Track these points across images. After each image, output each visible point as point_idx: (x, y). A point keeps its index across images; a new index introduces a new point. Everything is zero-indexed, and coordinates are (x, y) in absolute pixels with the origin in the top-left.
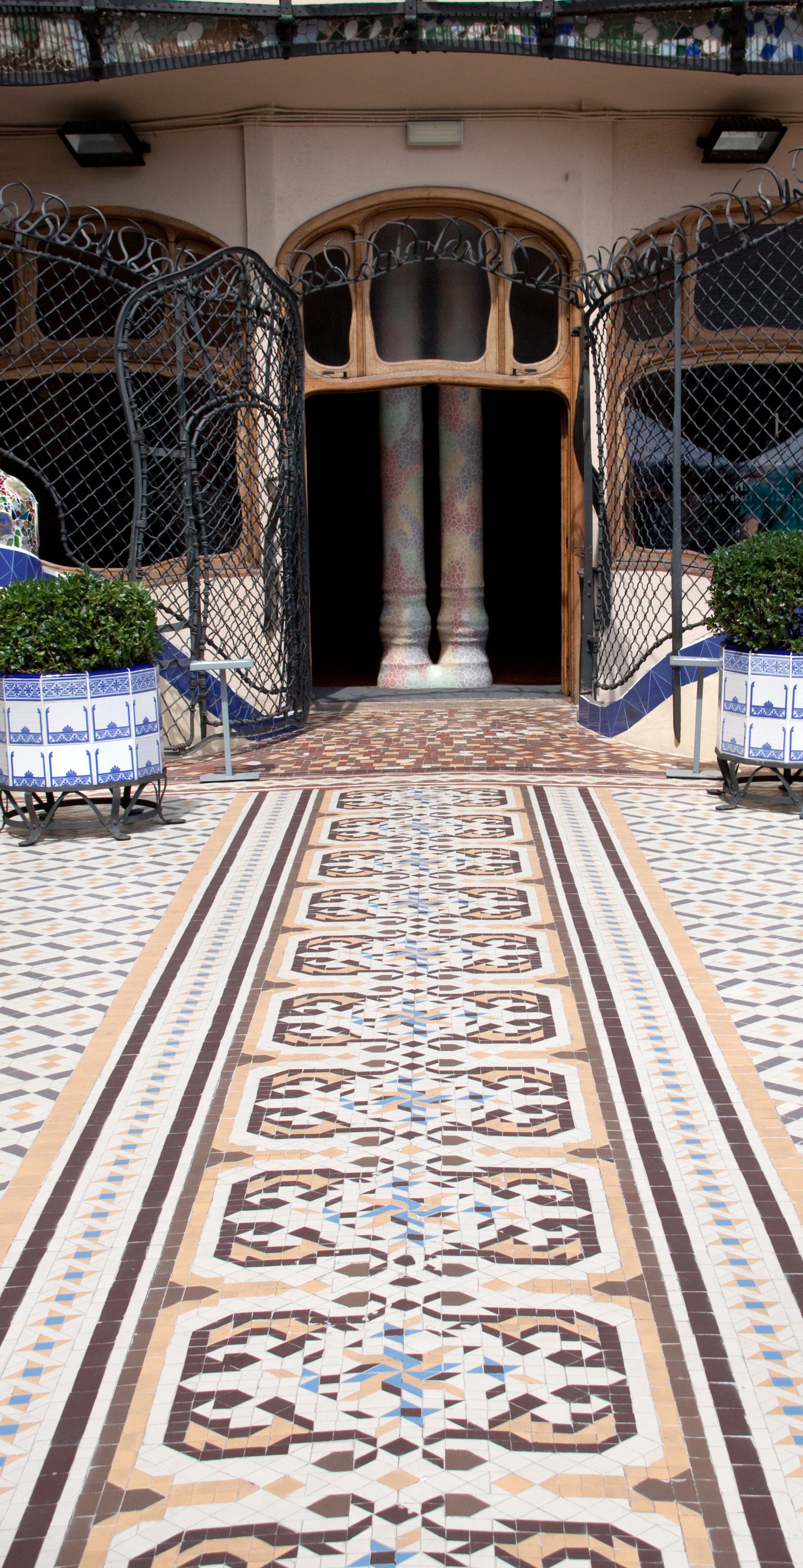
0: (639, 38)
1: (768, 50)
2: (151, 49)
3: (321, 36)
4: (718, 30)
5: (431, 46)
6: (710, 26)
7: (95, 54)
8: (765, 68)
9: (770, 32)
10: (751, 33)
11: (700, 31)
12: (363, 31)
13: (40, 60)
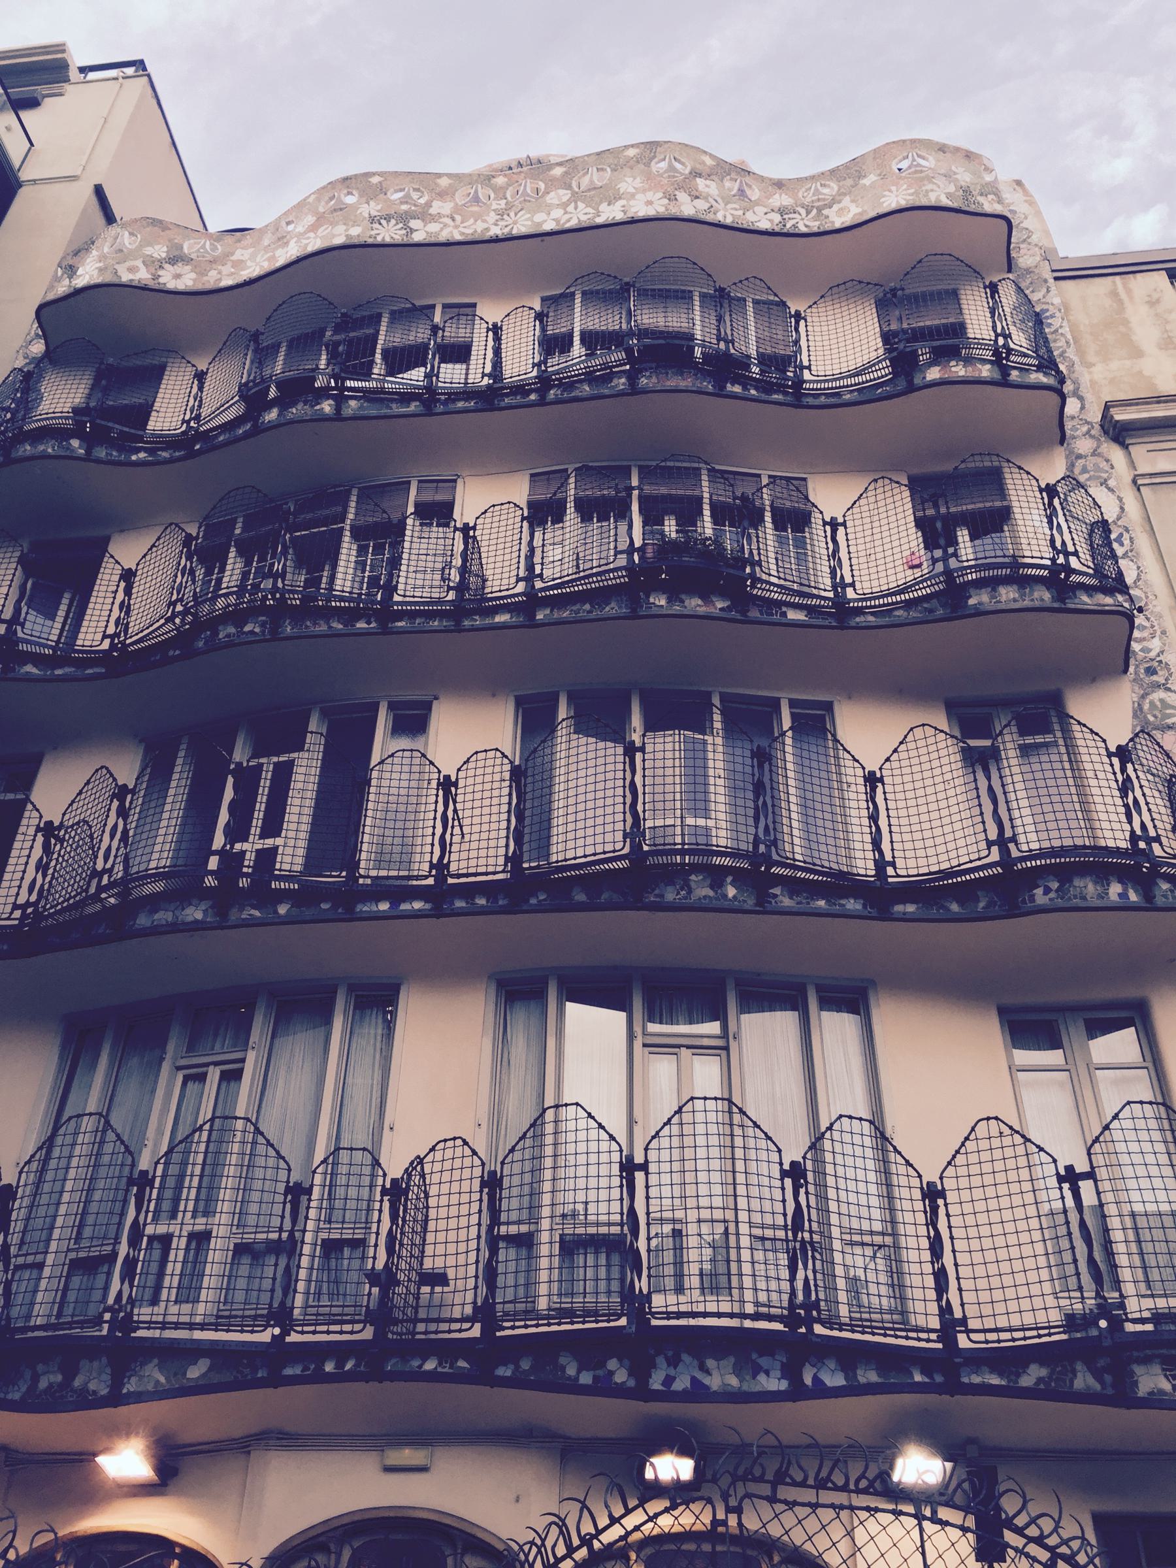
0: (563, 1368)
1: (668, 1381)
2: (162, 1379)
3: (305, 1369)
4: (626, 1362)
5: (394, 1376)
6: (620, 1360)
7: (117, 1383)
8: (668, 1395)
9: (669, 1365)
10: (654, 1366)
11: (612, 1364)
12: (340, 1365)
13: (72, 1390)
